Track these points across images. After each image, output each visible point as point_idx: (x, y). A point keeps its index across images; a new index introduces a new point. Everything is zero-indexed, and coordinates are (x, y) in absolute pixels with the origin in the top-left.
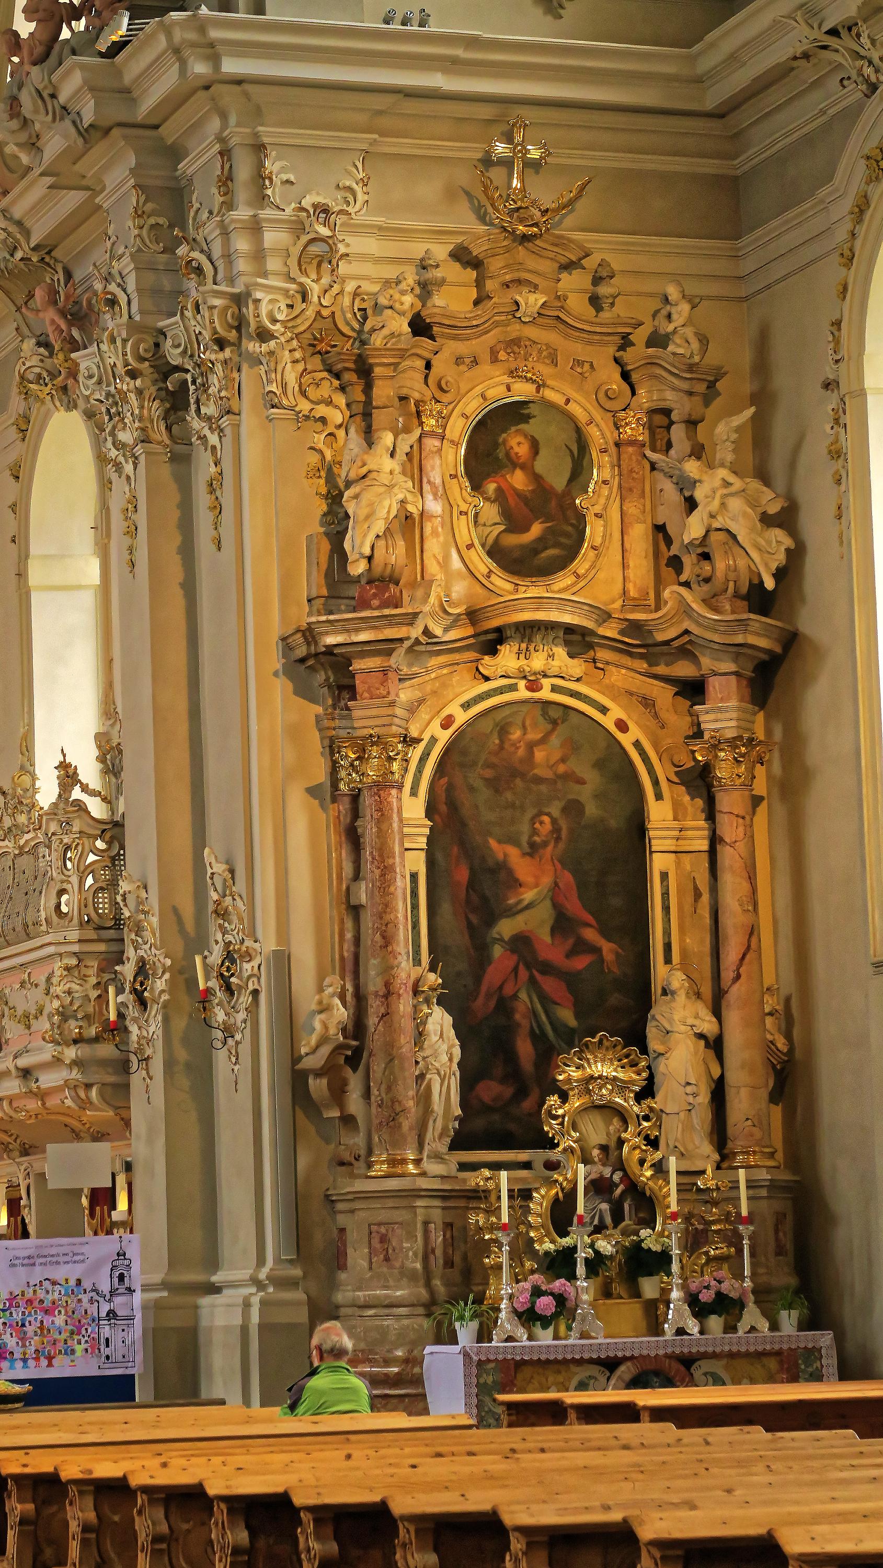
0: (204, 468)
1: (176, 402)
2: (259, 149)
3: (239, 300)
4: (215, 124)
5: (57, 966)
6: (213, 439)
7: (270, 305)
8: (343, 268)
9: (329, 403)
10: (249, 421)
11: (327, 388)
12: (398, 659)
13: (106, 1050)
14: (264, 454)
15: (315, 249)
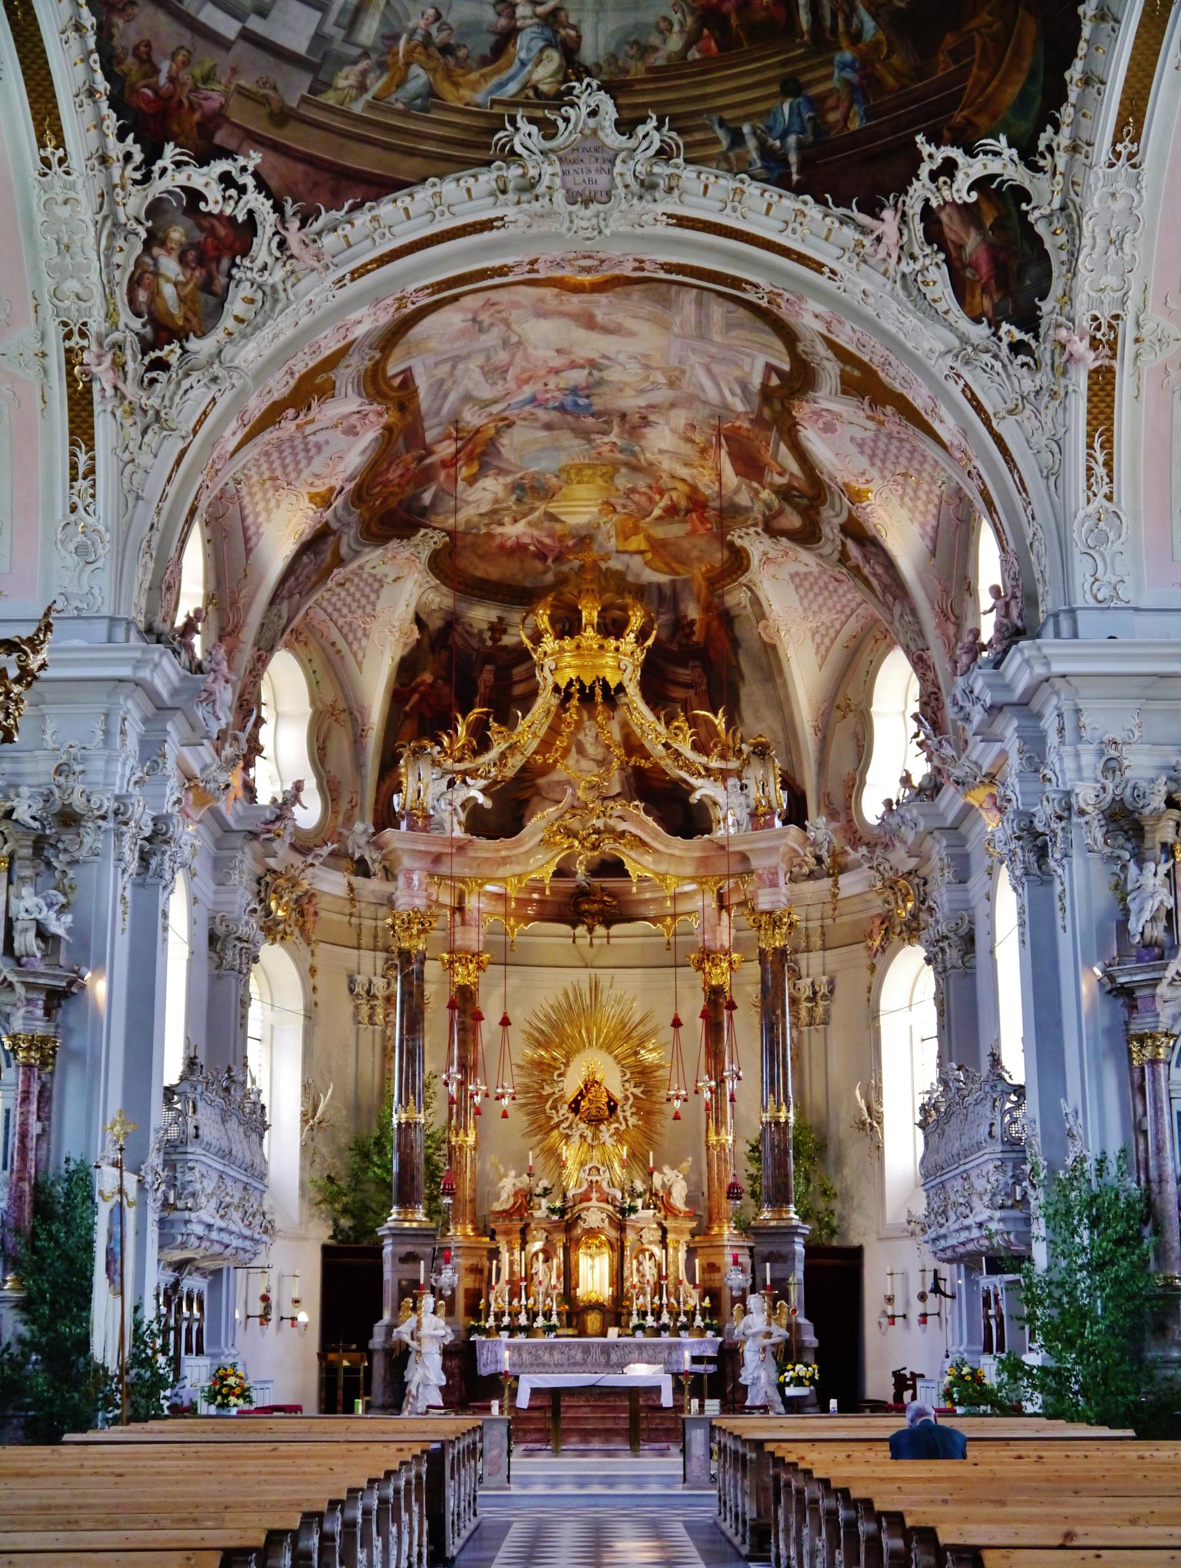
0: (1058, 888)
1: (1042, 853)
2: (1078, 711)
3: (1068, 794)
4: (1054, 701)
5: (991, 1167)
6: (1060, 871)
7: (1086, 794)
8: (1128, 773)
9: (1122, 848)
10: (1077, 860)
11: (1121, 840)
12: (1162, 989)
13: (1015, 1213)
14: (1081, 876)
15: (1113, 764)
